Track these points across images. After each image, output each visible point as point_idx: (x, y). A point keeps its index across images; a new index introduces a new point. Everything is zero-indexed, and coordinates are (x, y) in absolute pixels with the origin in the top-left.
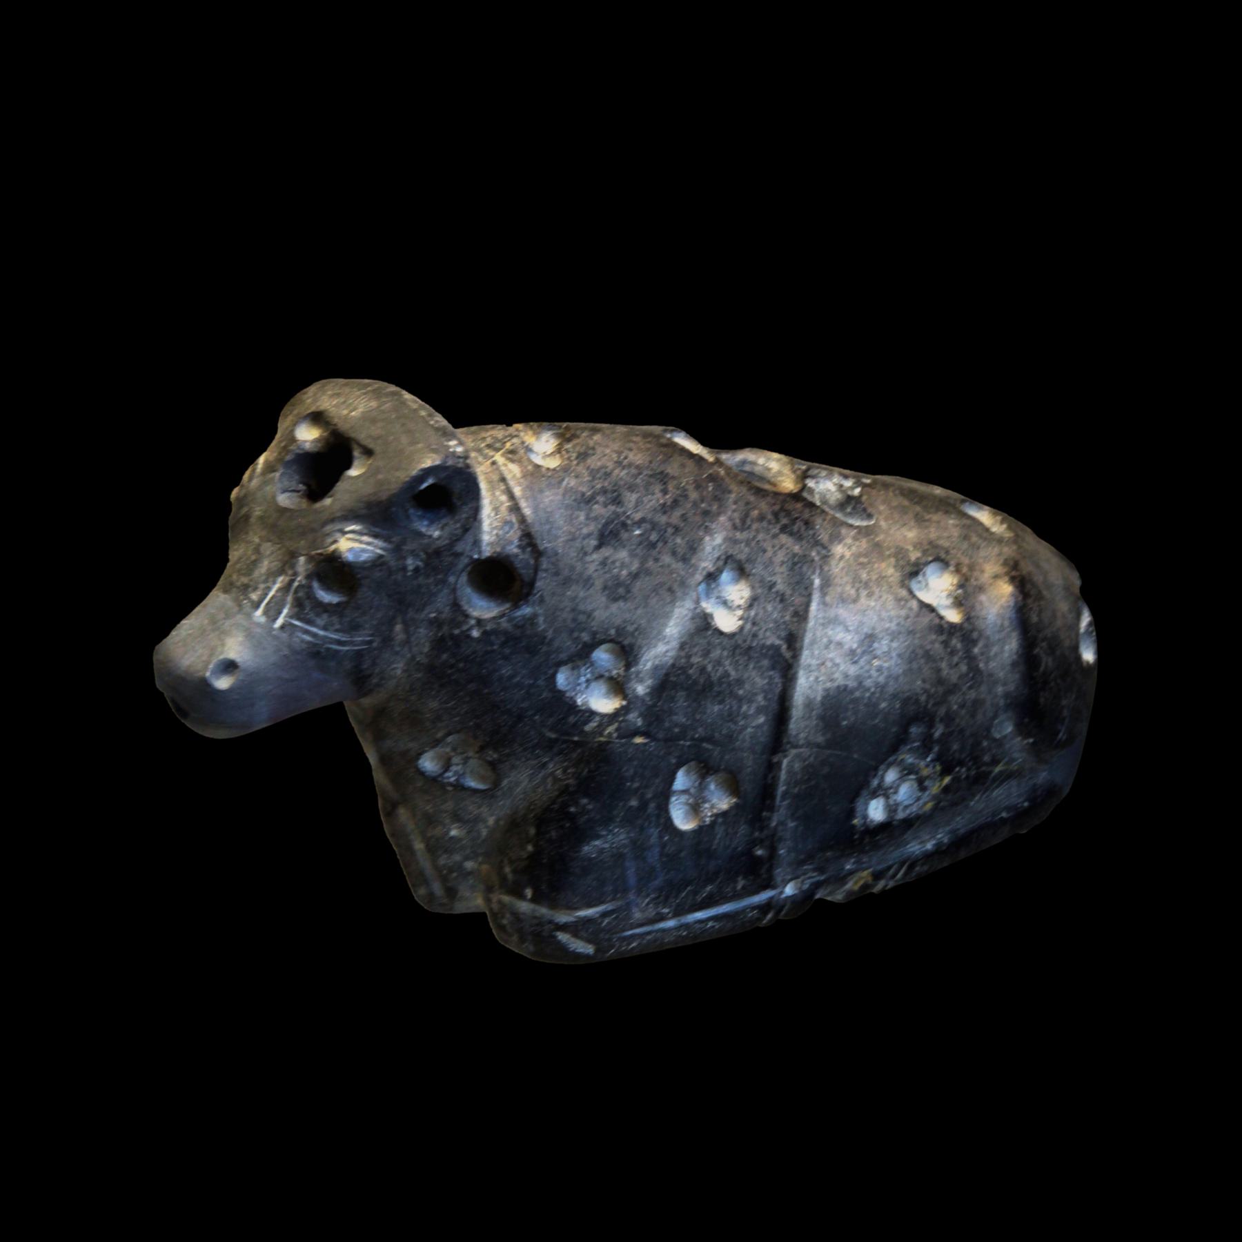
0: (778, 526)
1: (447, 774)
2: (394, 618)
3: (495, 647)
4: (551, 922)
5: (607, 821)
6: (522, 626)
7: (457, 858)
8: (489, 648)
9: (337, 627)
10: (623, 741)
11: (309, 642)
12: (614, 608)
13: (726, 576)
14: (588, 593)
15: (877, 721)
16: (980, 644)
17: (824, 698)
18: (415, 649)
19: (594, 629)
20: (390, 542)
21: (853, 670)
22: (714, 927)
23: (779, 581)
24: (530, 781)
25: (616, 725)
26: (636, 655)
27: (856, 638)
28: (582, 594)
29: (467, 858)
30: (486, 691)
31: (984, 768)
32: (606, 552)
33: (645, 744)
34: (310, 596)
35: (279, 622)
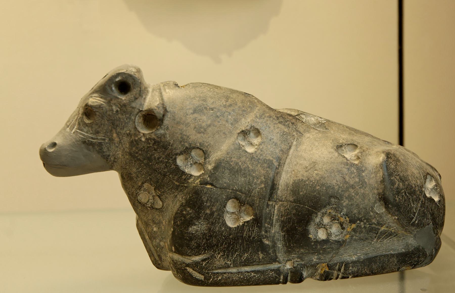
0: (278, 121)
1: (148, 204)
2: (111, 131)
3: (151, 145)
4: (184, 263)
5: (198, 218)
6: (160, 138)
7: (158, 241)
8: (149, 145)
9: (91, 132)
10: (202, 186)
11: (82, 138)
12: (199, 135)
13: (252, 134)
14: (187, 129)
15: (315, 193)
16: (366, 172)
17: (293, 183)
18: (124, 146)
19: (191, 142)
20: (107, 100)
21: (305, 174)
22: (255, 276)
23: (275, 138)
24: (172, 203)
25: (200, 180)
26: (209, 155)
27: (308, 163)
28: (185, 128)
29: (160, 241)
30: (151, 164)
31: (373, 226)
32: (196, 115)
33: (211, 188)
34: (82, 121)
35: (73, 131)
